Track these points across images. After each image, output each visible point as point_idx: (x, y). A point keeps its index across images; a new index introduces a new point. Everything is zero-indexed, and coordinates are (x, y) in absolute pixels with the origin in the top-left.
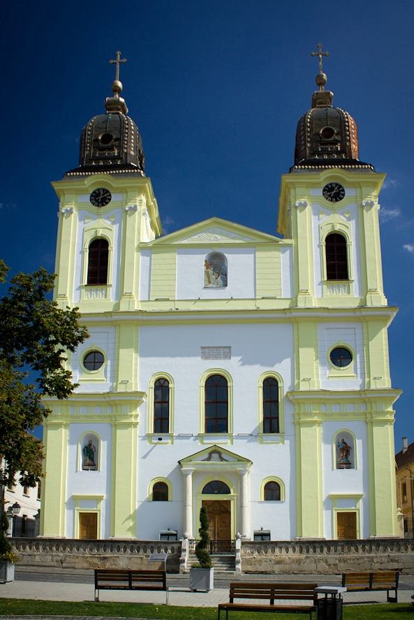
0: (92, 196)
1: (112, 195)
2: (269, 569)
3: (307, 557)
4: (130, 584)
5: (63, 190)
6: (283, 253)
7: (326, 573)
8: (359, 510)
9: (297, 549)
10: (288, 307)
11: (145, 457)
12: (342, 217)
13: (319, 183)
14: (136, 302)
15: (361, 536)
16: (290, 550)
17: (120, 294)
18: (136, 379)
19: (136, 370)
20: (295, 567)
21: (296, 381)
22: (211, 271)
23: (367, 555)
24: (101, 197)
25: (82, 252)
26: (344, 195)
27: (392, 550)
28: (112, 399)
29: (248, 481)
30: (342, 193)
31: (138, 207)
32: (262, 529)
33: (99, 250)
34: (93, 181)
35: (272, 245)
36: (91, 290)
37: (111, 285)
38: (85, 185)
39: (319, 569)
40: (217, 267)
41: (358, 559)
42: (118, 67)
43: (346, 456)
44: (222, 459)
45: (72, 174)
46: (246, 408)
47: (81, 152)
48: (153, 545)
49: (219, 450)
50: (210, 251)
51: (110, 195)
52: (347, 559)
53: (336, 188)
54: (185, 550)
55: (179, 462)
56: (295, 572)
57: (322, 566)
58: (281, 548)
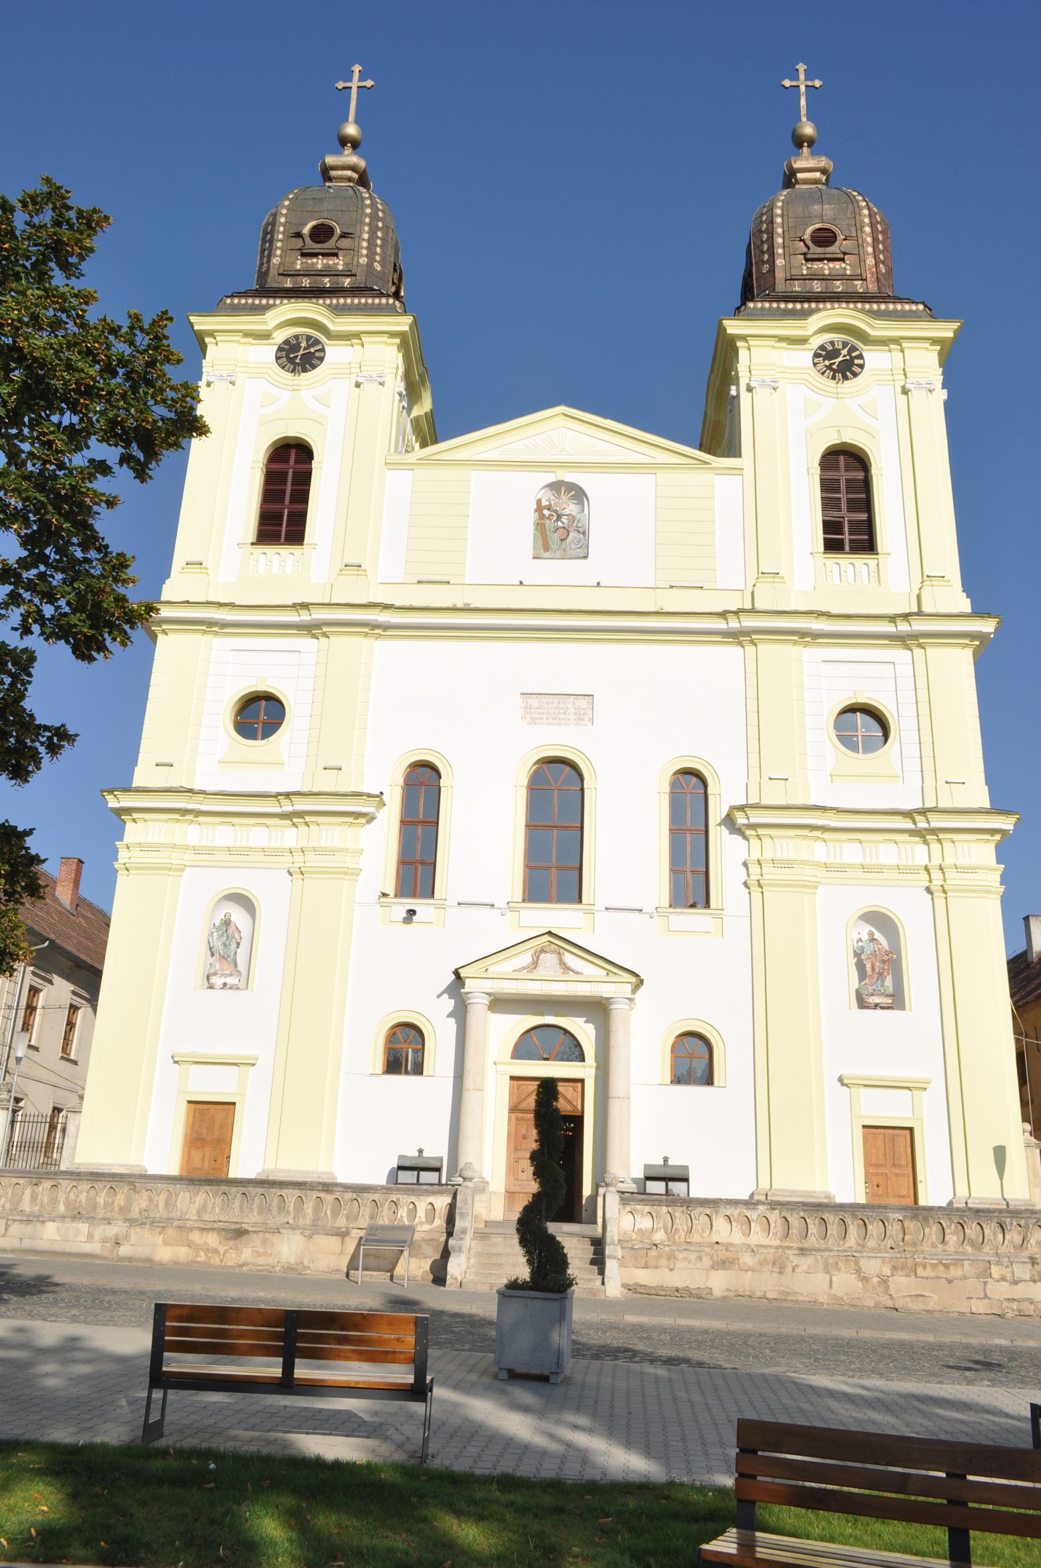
0: (280, 349)
1: (327, 349)
24: (302, 352)
26: (862, 366)
30: (856, 361)
33: (289, 469)
34: (282, 316)
41: (946, 1267)
45: (236, 301)
48: (376, 1197)
50: (551, 478)
51: (323, 350)
53: (844, 352)
55: (456, 973)
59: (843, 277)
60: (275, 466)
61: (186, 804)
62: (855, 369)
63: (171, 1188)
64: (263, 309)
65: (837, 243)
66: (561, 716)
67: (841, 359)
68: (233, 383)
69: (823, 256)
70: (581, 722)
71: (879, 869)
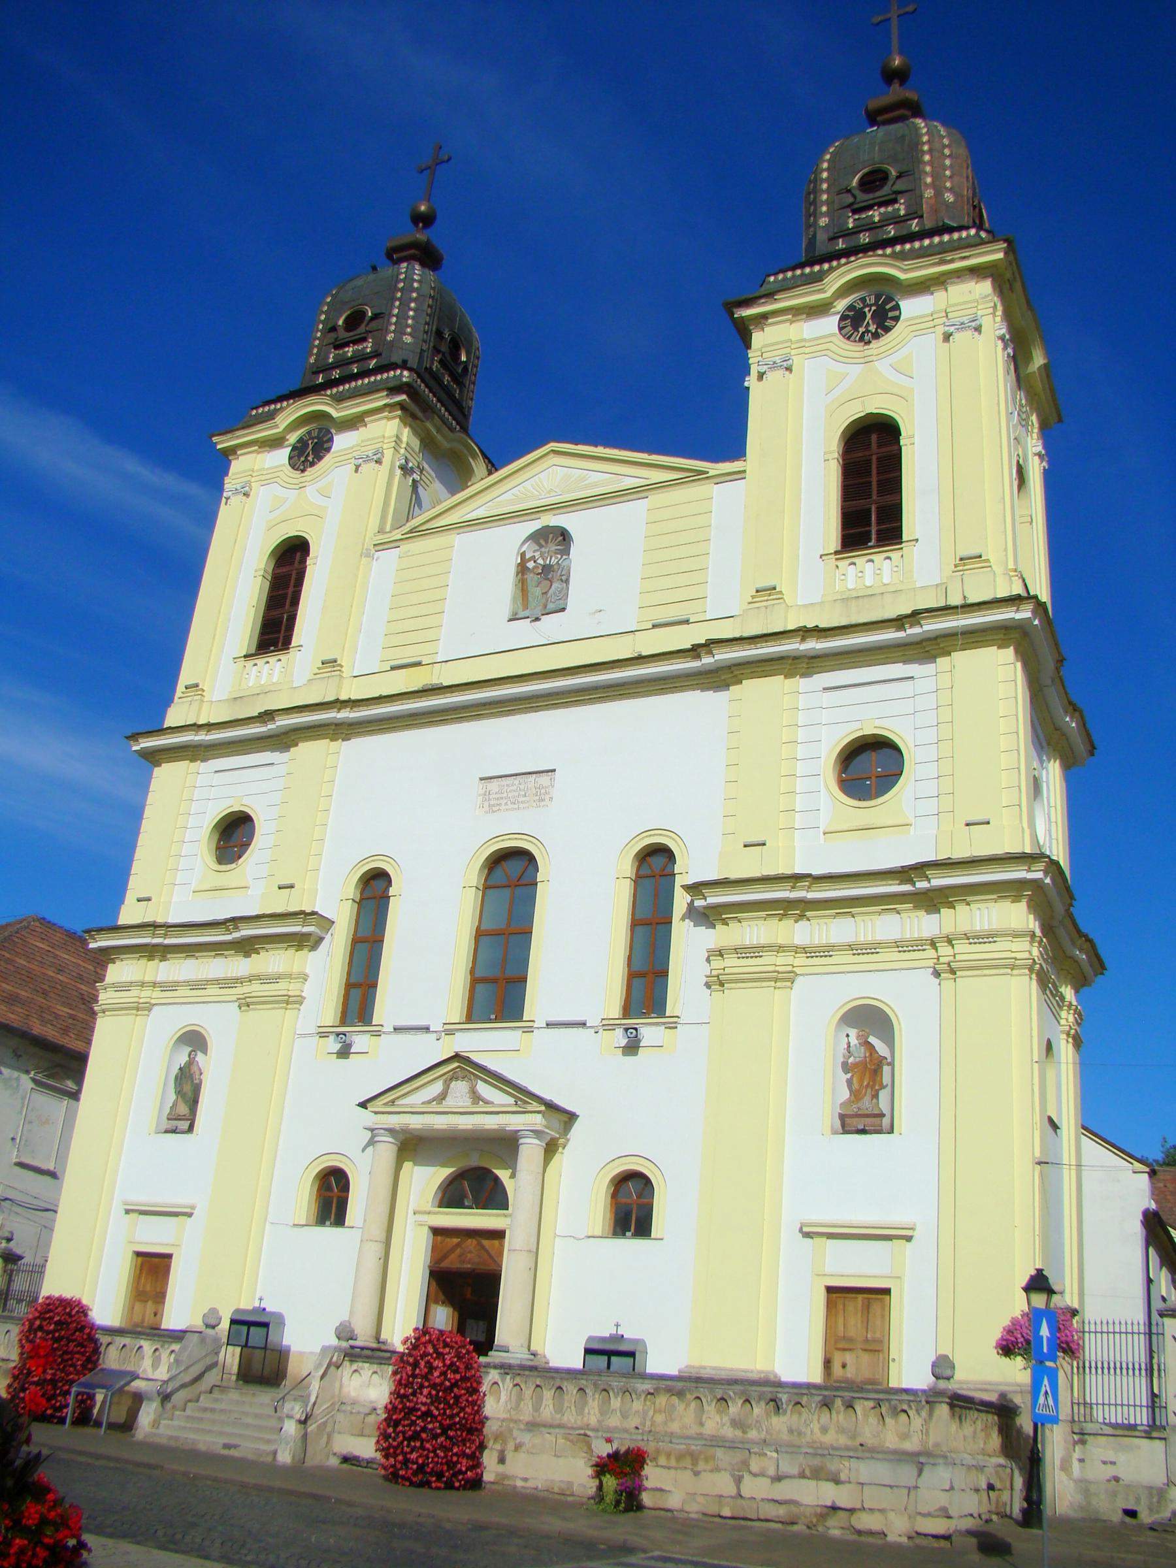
5: (233, 450)
46: (578, 941)
59: (897, 221)
61: (163, 942)
64: (271, 416)
65: (890, 183)
66: (521, 799)
67: (869, 316)
68: (246, 495)
69: (871, 202)
70: (542, 803)
71: (871, 948)
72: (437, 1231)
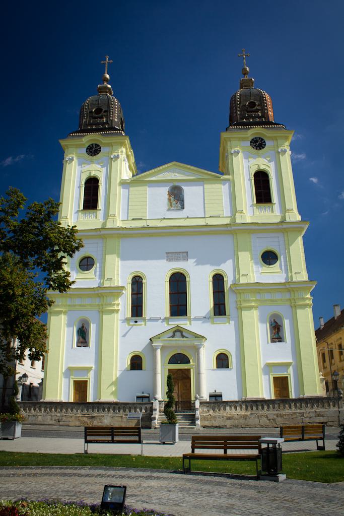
0: (87, 149)
2: (222, 424)
3: (252, 414)
4: (113, 438)
5: (67, 146)
6: (224, 185)
7: (267, 427)
8: (290, 374)
9: (244, 407)
10: (229, 223)
11: (124, 336)
12: (265, 160)
13: (248, 138)
14: (118, 221)
15: (293, 395)
16: (238, 408)
17: (107, 215)
18: (118, 277)
19: (118, 270)
20: (242, 421)
21: (237, 277)
22: (172, 198)
23: (298, 411)
24: (94, 149)
25: (80, 187)
26: (265, 145)
27: (318, 407)
28: (100, 291)
29: (203, 352)
31: (120, 156)
32: (215, 391)
33: (92, 185)
34: (88, 139)
35: (216, 180)
36: (90, 213)
37: (100, 210)
38: (82, 141)
39: (262, 423)
40: (177, 196)
41: (292, 415)
42: (107, 65)
43: (278, 333)
44: (183, 336)
45: (74, 134)
46: (200, 297)
47: (80, 119)
48: (131, 406)
49: (181, 329)
50: (172, 184)
51: (100, 148)
52: (283, 415)
54: (156, 410)
55: (150, 339)
56: (243, 426)
57: (264, 421)
58: (230, 406)
60: (86, 185)
62: (263, 146)
63: (72, 405)
71: (276, 301)
72: (170, 370)
